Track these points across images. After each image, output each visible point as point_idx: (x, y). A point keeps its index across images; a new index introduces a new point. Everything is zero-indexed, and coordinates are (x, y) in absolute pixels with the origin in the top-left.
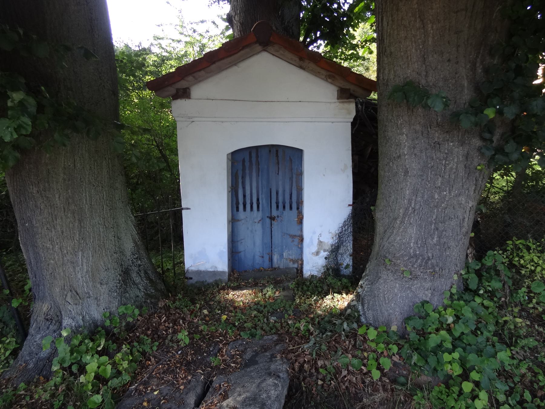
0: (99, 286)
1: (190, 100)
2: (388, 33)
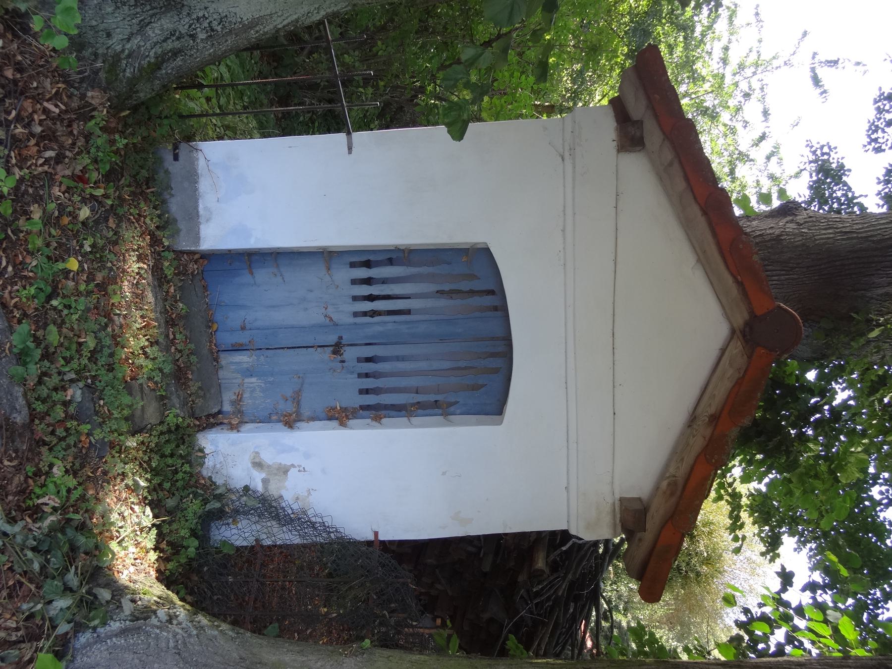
1: (615, 152)
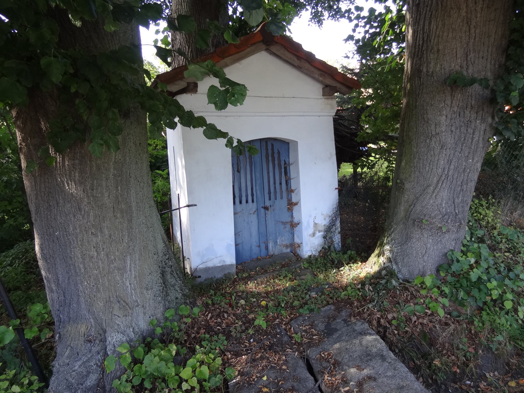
0: (145, 292)
1: (196, 95)
2: (437, 35)
